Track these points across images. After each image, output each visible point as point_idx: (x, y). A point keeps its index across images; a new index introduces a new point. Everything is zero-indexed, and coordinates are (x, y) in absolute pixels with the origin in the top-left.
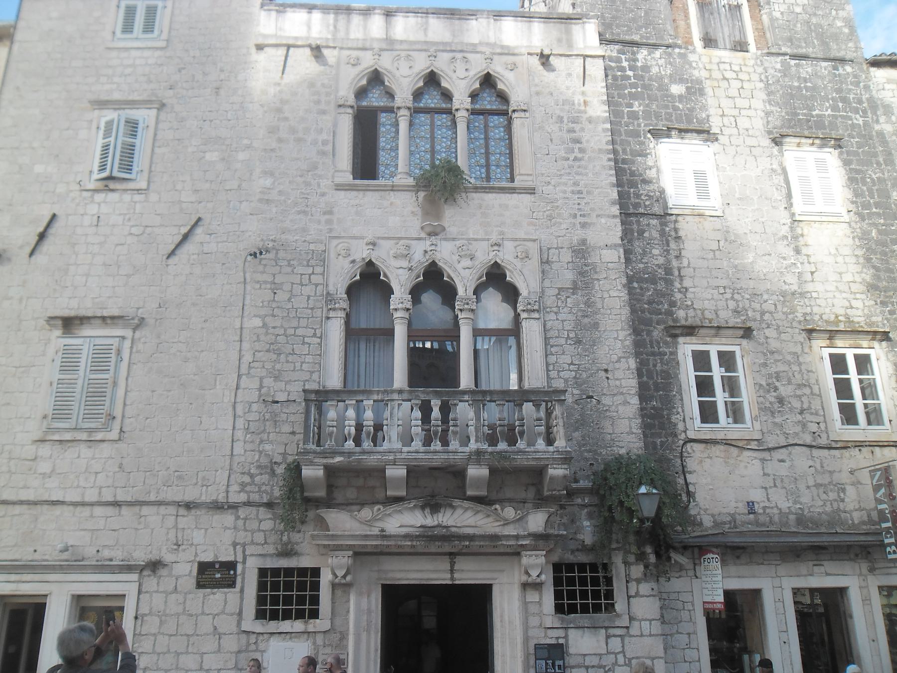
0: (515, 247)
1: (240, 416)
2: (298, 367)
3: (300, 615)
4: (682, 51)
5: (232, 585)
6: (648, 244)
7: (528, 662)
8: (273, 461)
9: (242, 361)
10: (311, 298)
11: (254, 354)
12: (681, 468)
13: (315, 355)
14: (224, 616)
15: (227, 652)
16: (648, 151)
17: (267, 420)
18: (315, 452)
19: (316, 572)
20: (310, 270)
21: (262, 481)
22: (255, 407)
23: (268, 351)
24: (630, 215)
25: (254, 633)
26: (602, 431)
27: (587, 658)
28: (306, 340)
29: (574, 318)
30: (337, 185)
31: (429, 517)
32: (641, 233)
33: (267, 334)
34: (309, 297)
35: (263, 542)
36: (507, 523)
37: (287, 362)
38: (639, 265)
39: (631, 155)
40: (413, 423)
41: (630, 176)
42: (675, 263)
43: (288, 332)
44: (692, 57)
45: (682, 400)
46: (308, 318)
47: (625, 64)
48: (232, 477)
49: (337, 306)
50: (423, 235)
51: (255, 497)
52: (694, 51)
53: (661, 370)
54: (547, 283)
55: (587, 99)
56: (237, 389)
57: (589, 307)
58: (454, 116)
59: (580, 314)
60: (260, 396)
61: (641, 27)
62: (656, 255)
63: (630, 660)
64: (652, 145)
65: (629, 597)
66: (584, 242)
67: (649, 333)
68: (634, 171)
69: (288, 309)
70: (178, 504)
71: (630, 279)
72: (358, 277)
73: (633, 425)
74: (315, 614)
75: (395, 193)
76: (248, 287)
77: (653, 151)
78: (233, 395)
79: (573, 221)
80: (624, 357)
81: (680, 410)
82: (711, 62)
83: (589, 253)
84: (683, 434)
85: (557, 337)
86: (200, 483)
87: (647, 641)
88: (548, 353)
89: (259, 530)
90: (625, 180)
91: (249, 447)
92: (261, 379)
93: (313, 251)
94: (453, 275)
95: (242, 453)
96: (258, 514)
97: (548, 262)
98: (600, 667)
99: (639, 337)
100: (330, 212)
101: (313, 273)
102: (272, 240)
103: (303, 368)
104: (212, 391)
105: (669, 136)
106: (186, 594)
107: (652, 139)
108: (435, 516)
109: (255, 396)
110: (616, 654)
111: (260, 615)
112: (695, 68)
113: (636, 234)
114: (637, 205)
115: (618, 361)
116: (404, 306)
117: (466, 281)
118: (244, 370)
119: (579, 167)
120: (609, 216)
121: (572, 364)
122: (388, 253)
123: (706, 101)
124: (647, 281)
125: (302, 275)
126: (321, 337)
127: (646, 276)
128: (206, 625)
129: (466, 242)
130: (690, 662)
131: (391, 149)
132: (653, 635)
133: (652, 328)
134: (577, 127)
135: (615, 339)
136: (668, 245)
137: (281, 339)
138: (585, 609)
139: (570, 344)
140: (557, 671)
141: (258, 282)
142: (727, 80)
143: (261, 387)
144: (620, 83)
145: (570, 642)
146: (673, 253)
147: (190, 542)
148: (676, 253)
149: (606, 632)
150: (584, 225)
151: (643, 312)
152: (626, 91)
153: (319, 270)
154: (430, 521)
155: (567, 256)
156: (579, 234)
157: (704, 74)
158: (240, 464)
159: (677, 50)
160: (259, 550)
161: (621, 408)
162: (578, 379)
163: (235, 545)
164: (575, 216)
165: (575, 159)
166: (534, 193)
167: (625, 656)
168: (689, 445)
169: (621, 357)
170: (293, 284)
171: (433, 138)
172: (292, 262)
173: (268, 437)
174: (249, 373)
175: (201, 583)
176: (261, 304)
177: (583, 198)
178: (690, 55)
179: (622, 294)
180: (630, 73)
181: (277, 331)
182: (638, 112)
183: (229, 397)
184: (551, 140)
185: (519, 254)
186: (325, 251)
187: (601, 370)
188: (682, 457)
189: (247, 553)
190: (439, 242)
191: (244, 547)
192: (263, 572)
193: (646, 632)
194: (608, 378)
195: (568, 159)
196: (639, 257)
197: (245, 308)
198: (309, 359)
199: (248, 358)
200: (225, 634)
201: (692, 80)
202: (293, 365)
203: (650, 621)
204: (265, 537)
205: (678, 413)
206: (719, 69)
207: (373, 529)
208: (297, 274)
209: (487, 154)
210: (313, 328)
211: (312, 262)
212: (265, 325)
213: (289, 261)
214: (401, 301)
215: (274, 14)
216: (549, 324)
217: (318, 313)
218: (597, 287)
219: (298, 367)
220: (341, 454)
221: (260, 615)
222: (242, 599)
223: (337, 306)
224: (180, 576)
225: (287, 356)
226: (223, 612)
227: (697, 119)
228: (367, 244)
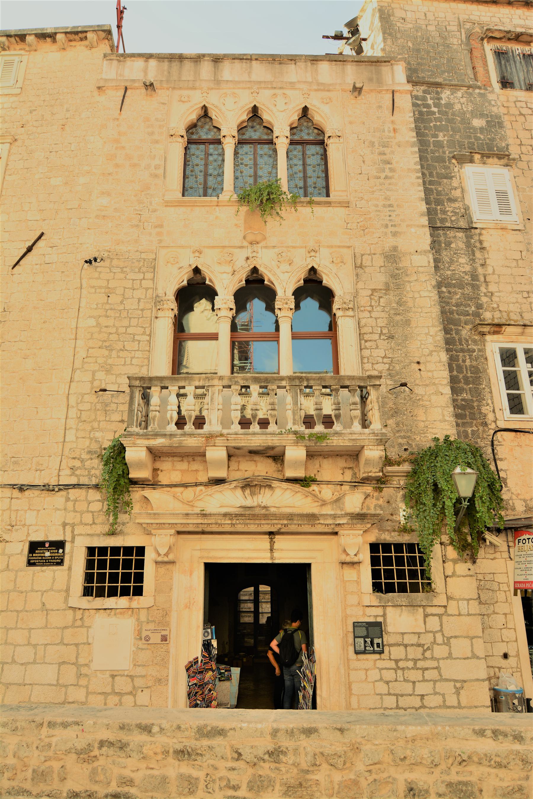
0: (331, 254)
1: (73, 407)
2: (128, 362)
3: (125, 592)
4: (482, 91)
5: (60, 563)
6: (455, 254)
7: (347, 640)
8: (103, 447)
9: (76, 356)
10: (142, 300)
11: (88, 350)
12: (492, 455)
13: (144, 351)
14: (53, 593)
15: (54, 628)
16: (453, 174)
18: (138, 434)
19: (141, 551)
20: (141, 276)
21: (92, 466)
22: (87, 398)
24: (437, 228)
26: (415, 418)
27: (405, 636)
28: (137, 337)
29: (387, 316)
30: (167, 202)
31: (249, 498)
32: (448, 244)
33: (100, 332)
34: (139, 300)
35: (91, 523)
36: (324, 503)
37: (118, 357)
38: (447, 272)
39: (438, 177)
40: (233, 407)
41: (437, 195)
42: (480, 270)
43: (119, 331)
44: (491, 97)
45: (491, 392)
46: (139, 318)
47: (430, 102)
48: (64, 461)
50: (245, 244)
51: (84, 480)
52: (492, 92)
53: (470, 366)
55: (395, 126)
57: (400, 306)
59: (392, 312)
61: (444, 72)
62: (463, 264)
63: (449, 639)
64: (456, 170)
65: (446, 577)
66: (395, 248)
67: (458, 332)
68: (441, 191)
69: (120, 311)
70: (13, 486)
71: (439, 285)
73: (446, 413)
74: (139, 592)
75: (220, 208)
77: (458, 174)
78: (67, 387)
79: (385, 230)
80: (435, 351)
81: (489, 402)
82: (508, 101)
83: (400, 258)
84: (493, 424)
85: (371, 333)
86: (34, 468)
87: (467, 619)
89: (88, 511)
90: (432, 199)
91: (81, 434)
92: (94, 373)
93: (144, 260)
94: (273, 279)
95: (75, 441)
96: (87, 496)
97: (361, 267)
98: (419, 645)
99: (448, 336)
100: (161, 226)
101: (144, 279)
102: (107, 251)
103: (133, 363)
105: (472, 161)
106: (17, 571)
107: (456, 164)
108: (255, 498)
109: (87, 388)
110: (434, 633)
111: (87, 592)
112: (494, 106)
113: (443, 245)
114: (443, 220)
115: (430, 354)
118: (78, 364)
119: (390, 184)
120: (418, 226)
121: (385, 357)
123: (505, 132)
124: (454, 286)
125: (133, 280)
127: (454, 282)
130: (507, 642)
132: (471, 615)
133: (460, 328)
134: (387, 150)
135: (427, 334)
136: (474, 255)
137: (113, 337)
138: (402, 589)
139: (384, 340)
140: (376, 649)
141: (94, 287)
142: (524, 115)
143: (93, 380)
144: (425, 117)
145: (389, 620)
146: (479, 262)
147: (23, 523)
148: (482, 262)
149: (424, 611)
150: (395, 234)
151: (452, 312)
152: (432, 124)
153: (149, 275)
154: (249, 502)
155: (379, 261)
156: (390, 242)
157: (503, 110)
158: (72, 450)
159: (477, 91)
160: (88, 530)
161: (434, 398)
162: (392, 370)
163: (64, 525)
164: (386, 226)
165: (386, 177)
166: (349, 207)
167: (443, 635)
168: (499, 434)
169: (432, 351)
170: (125, 288)
171: (255, 164)
172: (125, 269)
173: (99, 425)
174: (83, 368)
175: (32, 561)
176: (95, 306)
177: (394, 211)
178: (489, 95)
179: (432, 295)
180: (435, 110)
182: (443, 141)
184: (364, 162)
185: (334, 260)
187: (414, 363)
188: (492, 445)
189: (75, 533)
191: (73, 527)
192: (91, 550)
193: (464, 611)
194: (420, 370)
195: (380, 178)
196: (447, 265)
197: (81, 310)
198: (138, 354)
199: (82, 354)
200: (52, 610)
201: (491, 116)
202: (123, 359)
203: (468, 600)
204: (93, 518)
205: (488, 405)
206: (516, 107)
207: (195, 509)
208: (129, 279)
210: (142, 327)
211: (144, 269)
212: (98, 324)
214: (225, 301)
215: (115, 63)
216: (363, 322)
217: (147, 313)
218: (408, 288)
219: (128, 362)
220: (165, 435)
221: (87, 592)
222: (69, 576)
223: (165, 306)
224: (12, 555)
226: (51, 589)
227: (497, 147)
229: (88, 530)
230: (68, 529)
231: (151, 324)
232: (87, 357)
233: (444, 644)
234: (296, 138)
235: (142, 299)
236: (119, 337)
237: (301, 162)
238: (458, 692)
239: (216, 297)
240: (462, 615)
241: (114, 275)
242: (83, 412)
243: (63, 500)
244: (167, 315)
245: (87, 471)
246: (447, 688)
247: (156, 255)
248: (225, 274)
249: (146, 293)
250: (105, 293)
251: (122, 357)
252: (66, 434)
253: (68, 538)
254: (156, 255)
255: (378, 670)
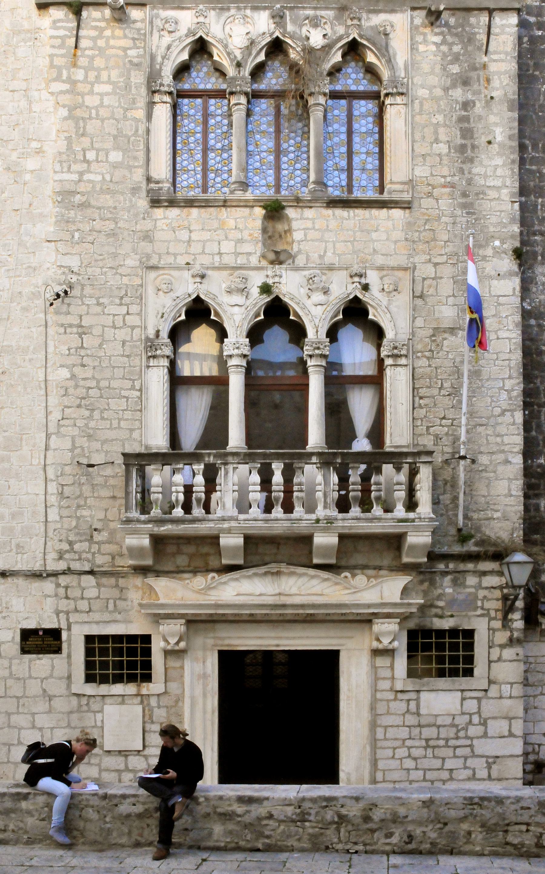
10: (127, 343)
14: (53, 680)
17: (83, 484)
23: (79, 406)
25: (84, 695)
28: (124, 393)
46: (124, 367)
49: (159, 352)
54: (419, 322)
56: (46, 449)
58: (307, 101)
60: (73, 458)
71: (526, 314)
72: (183, 317)
76: (51, 331)
88: (416, 405)
104: (18, 453)
116: (240, 352)
117: (317, 321)
118: (52, 428)
122: (220, 286)
126: (140, 390)
128: (34, 688)
129: (318, 272)
131: (222, 149)
158: (57, 531)
172: (101, 300)
175: (26, 649)
176: (67, 352)
181: (89, 384)
183: (38, 460)
186: (142, 286)
190: (284, 272)
209: (350, 154)
210: (130, 379)
213: (98, 299)
214: (237, 345)
216: (418, 371)
222: (70, 664)
223: (159, 352)
225: (102, 412)
228: (193, 276)
229: (84, 617)
230: (62, 616)
231: (141, 375)
232: (63, 419)
233: (480, 724)
234: (338, 88)
235: (128, 341)
236: (101, 393)
237: (344, 129)
238: (489, 767)
239: (225, 340)
240: (503, 698)
241: (88, 308)
242: (65, 487)
243: (53, 586)
244: (162, 364)
245: (77, 555)
246: (479, 764)
247: (142, 279)
248: (236, 308)
249: (132, 332)
250: (77, 333)
251: (107, 419)
252: (48, 513)
253: (64, 626)
254: (142, 279)
255: (406, 749)
